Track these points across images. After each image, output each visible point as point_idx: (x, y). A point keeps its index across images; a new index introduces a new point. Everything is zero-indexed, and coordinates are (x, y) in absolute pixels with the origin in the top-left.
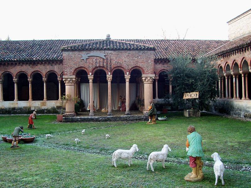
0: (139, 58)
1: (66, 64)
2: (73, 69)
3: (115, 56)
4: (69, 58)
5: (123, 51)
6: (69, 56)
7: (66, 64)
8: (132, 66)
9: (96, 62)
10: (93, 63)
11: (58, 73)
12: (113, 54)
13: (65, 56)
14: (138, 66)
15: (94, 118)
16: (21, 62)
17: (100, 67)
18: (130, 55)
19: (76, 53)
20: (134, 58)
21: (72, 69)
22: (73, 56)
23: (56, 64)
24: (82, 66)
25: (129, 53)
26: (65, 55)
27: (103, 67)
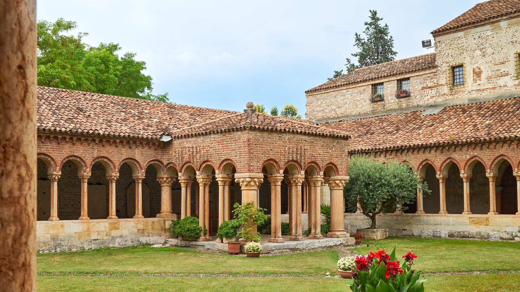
0: (334, 150)
1: (252, 153)
2: (262, 162)
3: (310, 144)
4: (256, 143)
5: (317, 138)
6: (257, 140)
7: (252, 153)
8: (327, 162)
9: (289, 153)
10: (286, 154)
11: (141, 163)
12: (306, 141)
13: (251, 139)
14: (333, 162)
15: (291, 245)
16: (75, 136)
17: (293, 161)
18: (325, 145)
19: (265, 134)
20: (328, 150)
21: (259, 162)
22: (261, 140)
23: (137, 147)
24: (272, 157)
25: (324, 142)
26: (251, 136)
27: (296, 161)
